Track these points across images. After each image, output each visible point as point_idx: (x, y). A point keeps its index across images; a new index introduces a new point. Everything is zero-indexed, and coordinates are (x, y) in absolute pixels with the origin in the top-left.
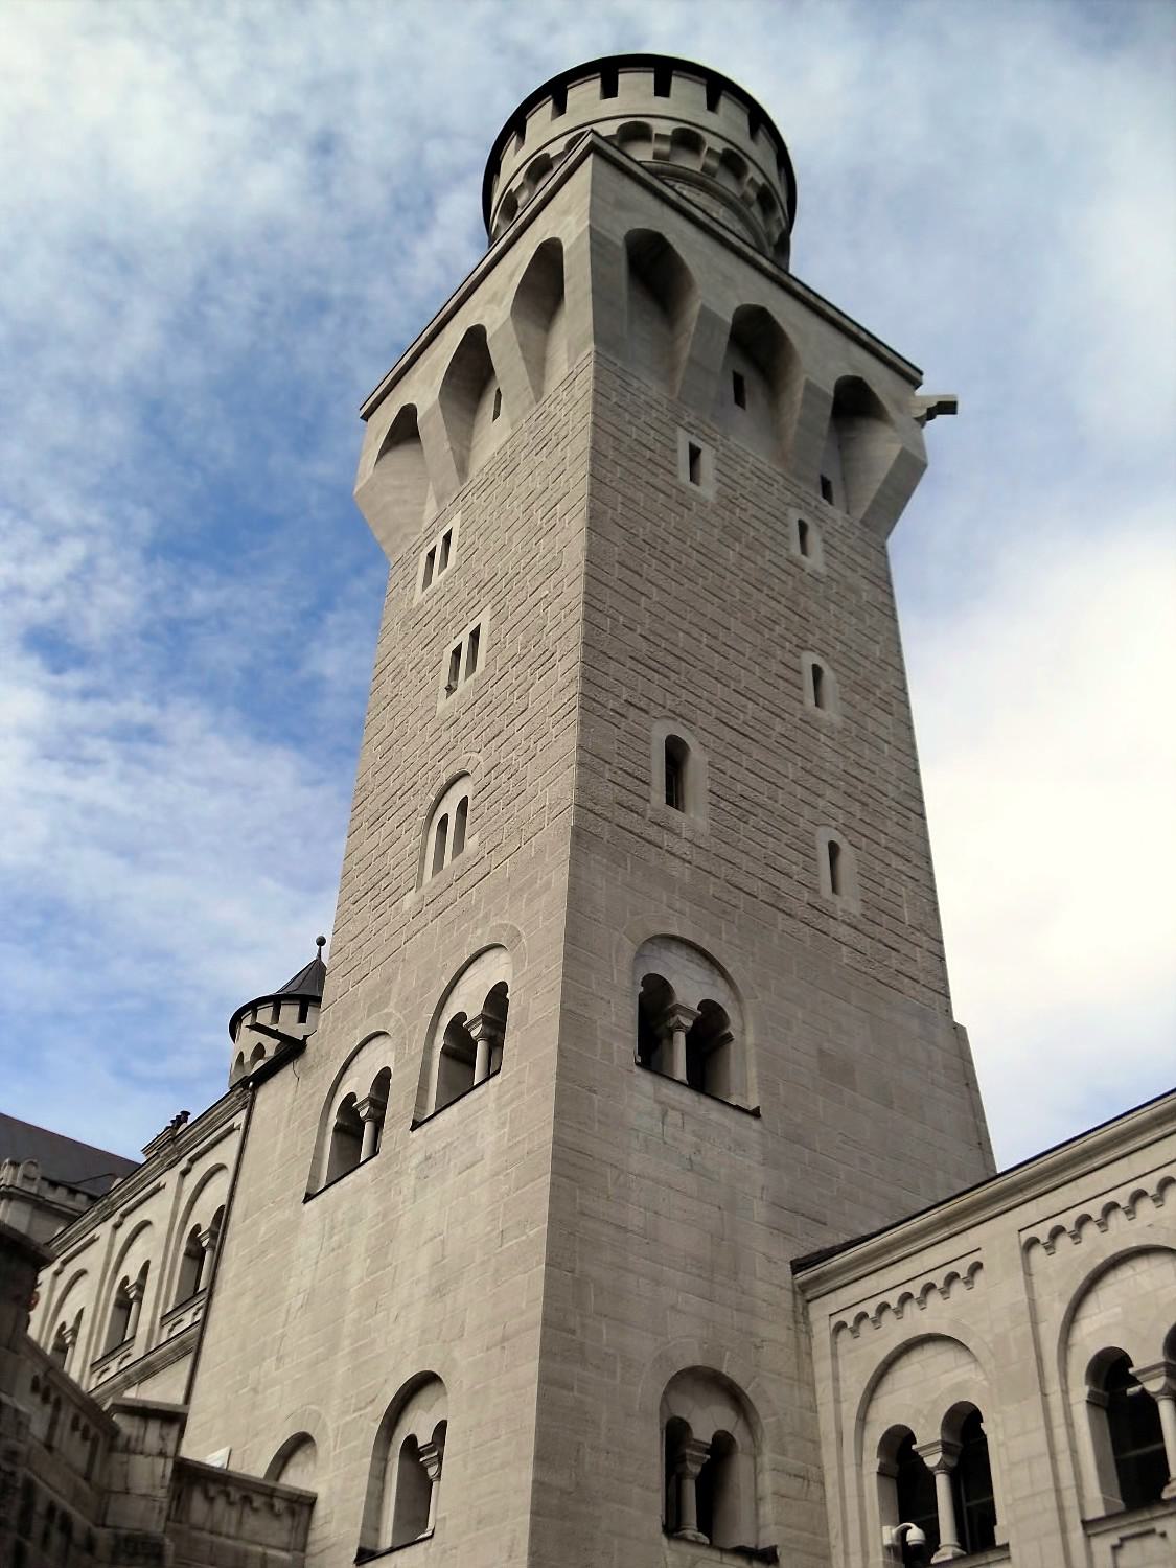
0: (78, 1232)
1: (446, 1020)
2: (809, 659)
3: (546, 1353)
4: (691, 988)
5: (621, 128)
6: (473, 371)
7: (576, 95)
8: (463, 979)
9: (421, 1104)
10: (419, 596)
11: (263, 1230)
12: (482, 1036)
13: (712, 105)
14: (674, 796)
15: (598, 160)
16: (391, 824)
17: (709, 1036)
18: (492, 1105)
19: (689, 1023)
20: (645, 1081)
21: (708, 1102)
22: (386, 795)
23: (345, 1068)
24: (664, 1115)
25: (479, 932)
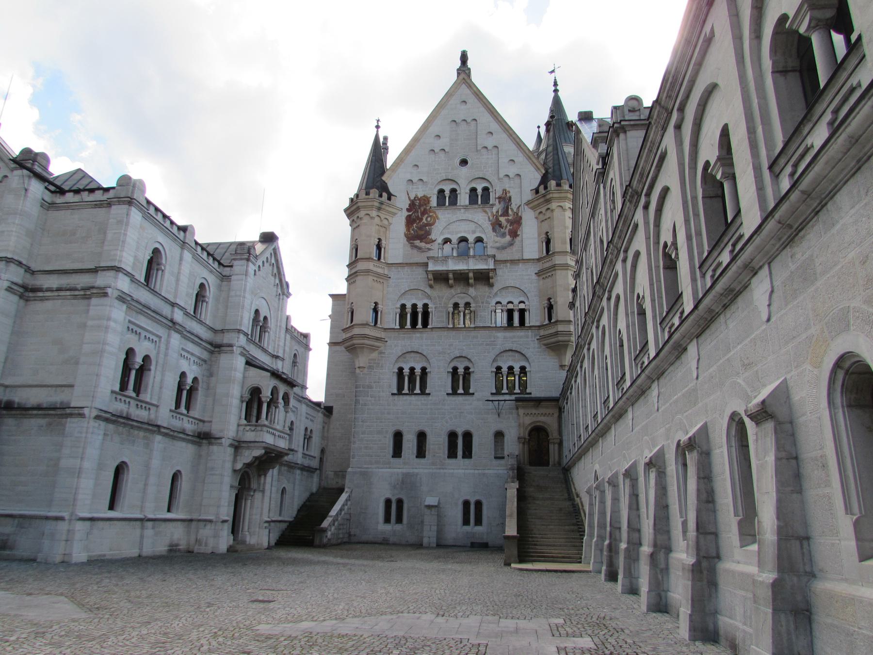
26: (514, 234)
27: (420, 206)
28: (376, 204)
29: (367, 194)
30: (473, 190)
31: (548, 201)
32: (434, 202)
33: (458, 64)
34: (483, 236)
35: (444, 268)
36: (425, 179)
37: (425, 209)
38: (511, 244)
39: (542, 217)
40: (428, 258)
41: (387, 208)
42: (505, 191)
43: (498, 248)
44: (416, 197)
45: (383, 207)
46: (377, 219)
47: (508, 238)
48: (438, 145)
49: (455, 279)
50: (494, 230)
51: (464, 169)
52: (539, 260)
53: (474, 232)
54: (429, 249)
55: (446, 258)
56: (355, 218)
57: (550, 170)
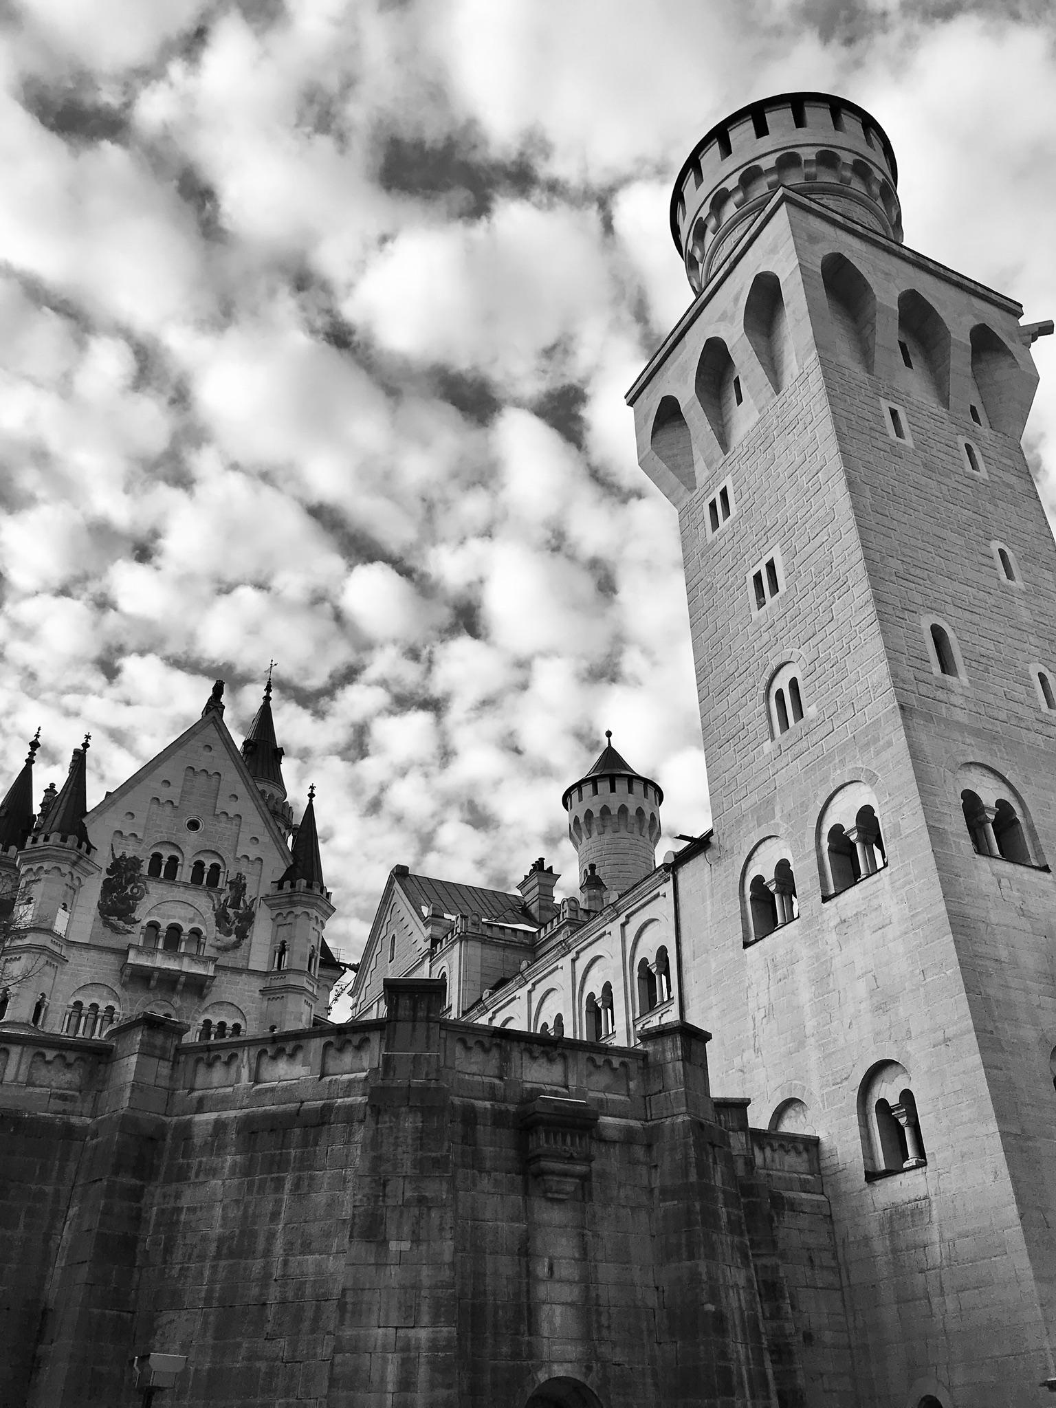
0: (543, 965)
1: (826, 830)
2: (996, 545)
3: (982, 1049)
4: (990, 793)
5: (779, 160)
6: (716, 368)
7: (735, 135)
8: (833, 802)
9: (824, 884)
10: (711, 536)
11: (713, 965)
12: (859, 839)
13: (837, 125)
14: (947, 665)
15: (790, 206)
16: (734, 695)
17: (1005, 819)
18: (888, 887)
19: (992, 817)
20: (983, 862)
21: (1021, 869)
22: (725, 675)
23: (749, 859)
24: (999, 882)
25: (839, 772)
26: (242, 935)
27: (127, 869)
28: (74, 858)
29: (64, 840)
30: (199, 865)
31: (293, 904)
32: (145, 870)
33: (210, 693)
34: (202, 928)
35: (149, 964)
36: (140, 835)
37: (133, 876)
38: (236, 946)
39: (280, 918)
40: (130, 946)
41: (84, 864)
42: (240, 876)
43: (218, 949)
44: (124, 854)
45: (81, 862)
46: (69, 876)
47: (233, 937)
48: (165, 794)
49: (159, 981)
50: (218, 924)
51: (193, 835)
52: (267, 974)
53: (192, 921)
54: (130, 932)
55: (153, 952)
56: (35, 867)
57: (299, 864)
